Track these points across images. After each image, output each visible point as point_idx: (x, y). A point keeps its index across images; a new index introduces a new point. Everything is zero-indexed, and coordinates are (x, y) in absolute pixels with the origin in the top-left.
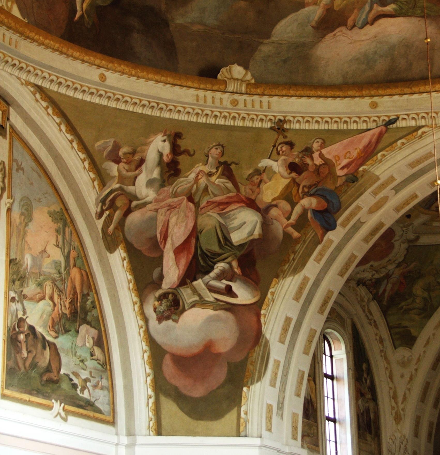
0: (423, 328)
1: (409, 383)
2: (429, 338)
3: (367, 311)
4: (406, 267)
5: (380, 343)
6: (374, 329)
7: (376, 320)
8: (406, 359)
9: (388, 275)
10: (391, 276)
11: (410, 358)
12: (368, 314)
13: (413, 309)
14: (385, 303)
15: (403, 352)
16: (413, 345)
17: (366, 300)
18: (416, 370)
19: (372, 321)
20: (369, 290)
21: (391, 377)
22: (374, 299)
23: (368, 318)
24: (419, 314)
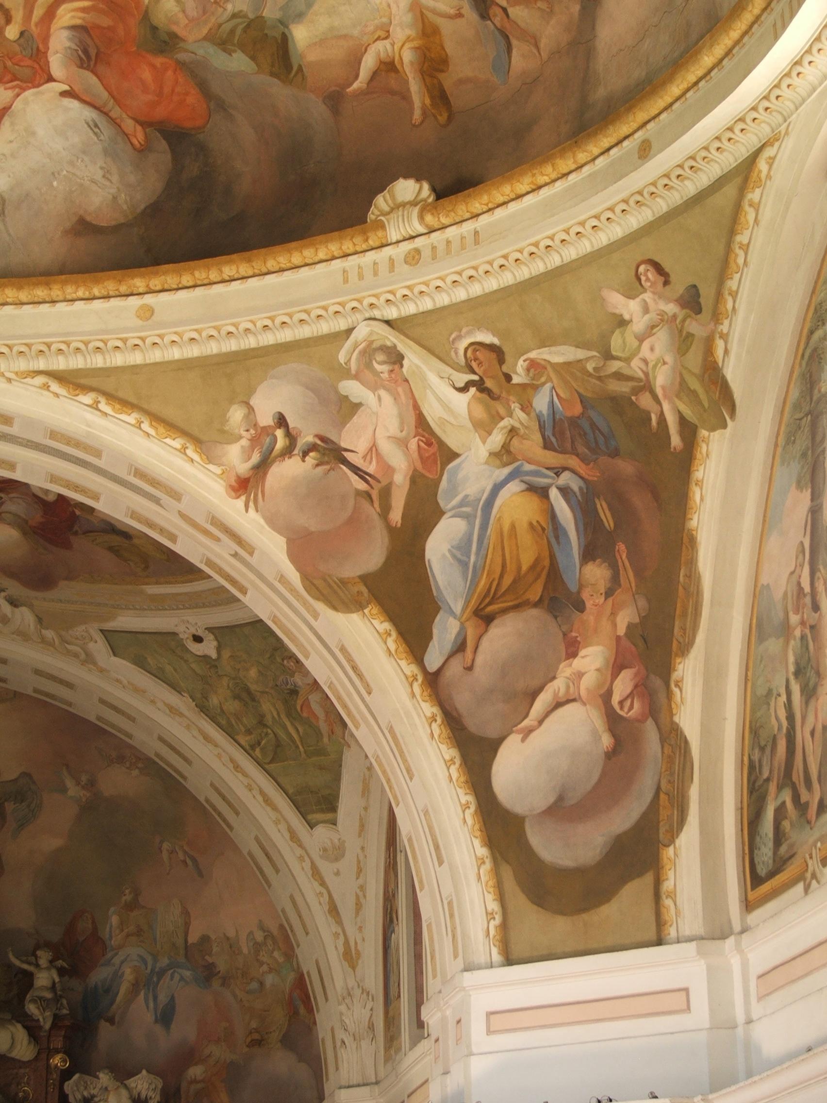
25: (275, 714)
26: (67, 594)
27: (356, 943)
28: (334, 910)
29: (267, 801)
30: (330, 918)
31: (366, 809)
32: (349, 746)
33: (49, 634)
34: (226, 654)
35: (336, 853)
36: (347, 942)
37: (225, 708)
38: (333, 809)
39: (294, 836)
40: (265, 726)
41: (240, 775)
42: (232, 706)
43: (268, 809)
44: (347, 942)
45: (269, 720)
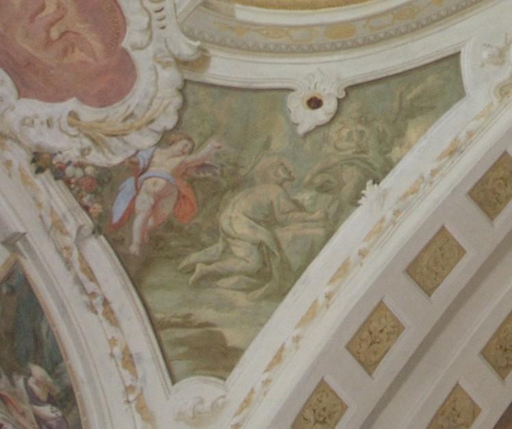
0: (262, 325)
2: (282, 349)
3: (77, 265)
4: (191, 152)
5: (125, 367)
6: (106, 324)
7: (109, 298)
8: (207, 405)
9: (137, 164)
10: (145, 170)
11: (220, 401)
12: (82, 276)
13: (229, 274)
14: (134, 249)
15: (198, 389)
16: (230, 369)
17: (71, 227)
19: (98, 301)
20: (78, 197)
22: (97, 231)
23: (83, 290)
24: (248, 290)
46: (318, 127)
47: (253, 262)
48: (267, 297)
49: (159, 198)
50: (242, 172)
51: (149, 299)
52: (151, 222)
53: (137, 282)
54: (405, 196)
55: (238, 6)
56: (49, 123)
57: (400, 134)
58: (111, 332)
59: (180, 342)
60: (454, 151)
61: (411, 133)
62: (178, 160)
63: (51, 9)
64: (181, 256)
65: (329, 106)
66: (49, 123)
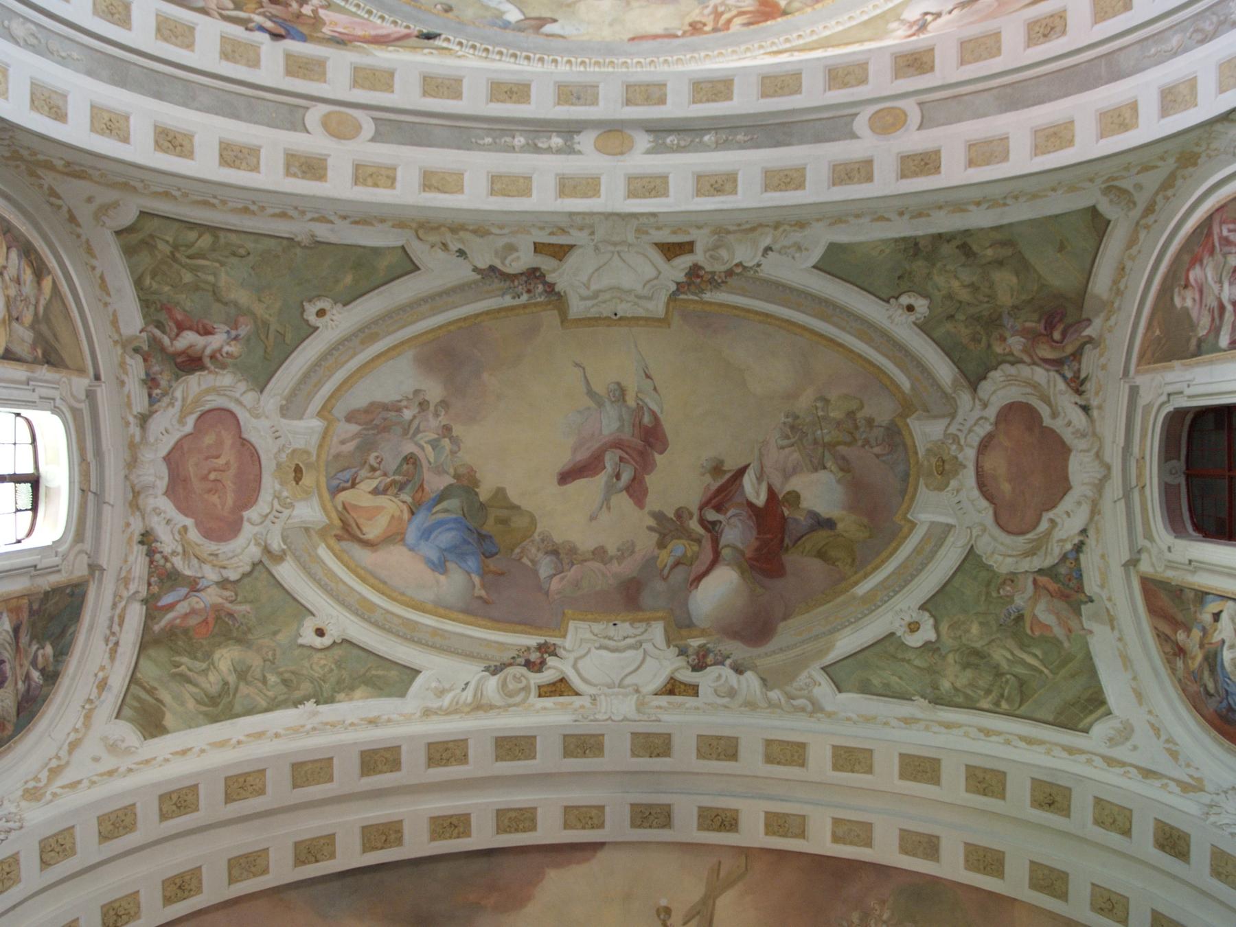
1: (102, 775)
2: (190, 749)
3: (118, 611)
4: (231, 602)
6: (107, 655)
7: (121, 643)
8: (123, 746)
10: (198, 591)
12: (116, 619)
13: (196, 685)
14: (156, 628)
15: (126, 732)
16: (153, 736)
17: (133, 587)
18: (130, 770)
19: (113, 639)
20: (150, 575)
21: (73, 746)
22: (145, 601)
23: (110, 627)
24: (198, 702)
25: (1010, 657)
26: (787, 633)
27: (1191, 776)
28: (1147, 773)
29: (1029, 741)
30: (1148, 781)
31: (1134, 678)
32: (1091, 632)
33: (775, 695)
34: (944, 627)
35: (1126, 732)
36: (1178, 782)
37: (958, 685)
38: (1103, 702)
39: (1071, 750)
40: (1003, 674)
41: (994, 738)
42: (965, 678)
43: (1034, 747)
44: (1178, 782)
45: (1005, 666)
46: (311, 647)
47: (214, 690)
48: (206, 714)
49: (193, 612)
50: (250, 637)
51: (141, 662)
52: (178, 621)
53: (143, 647)
54: (327, 724)
55: (323, 545)
56: (168, 522)
57: (352, 688)
58: (106, 662)
59: (138, 699)
60: (373, 722)
61: (358, 693)
62: (220, 600)
63: (221, 461)
64: (178, 653)
65: (327, 641)
66: (168, 522)
